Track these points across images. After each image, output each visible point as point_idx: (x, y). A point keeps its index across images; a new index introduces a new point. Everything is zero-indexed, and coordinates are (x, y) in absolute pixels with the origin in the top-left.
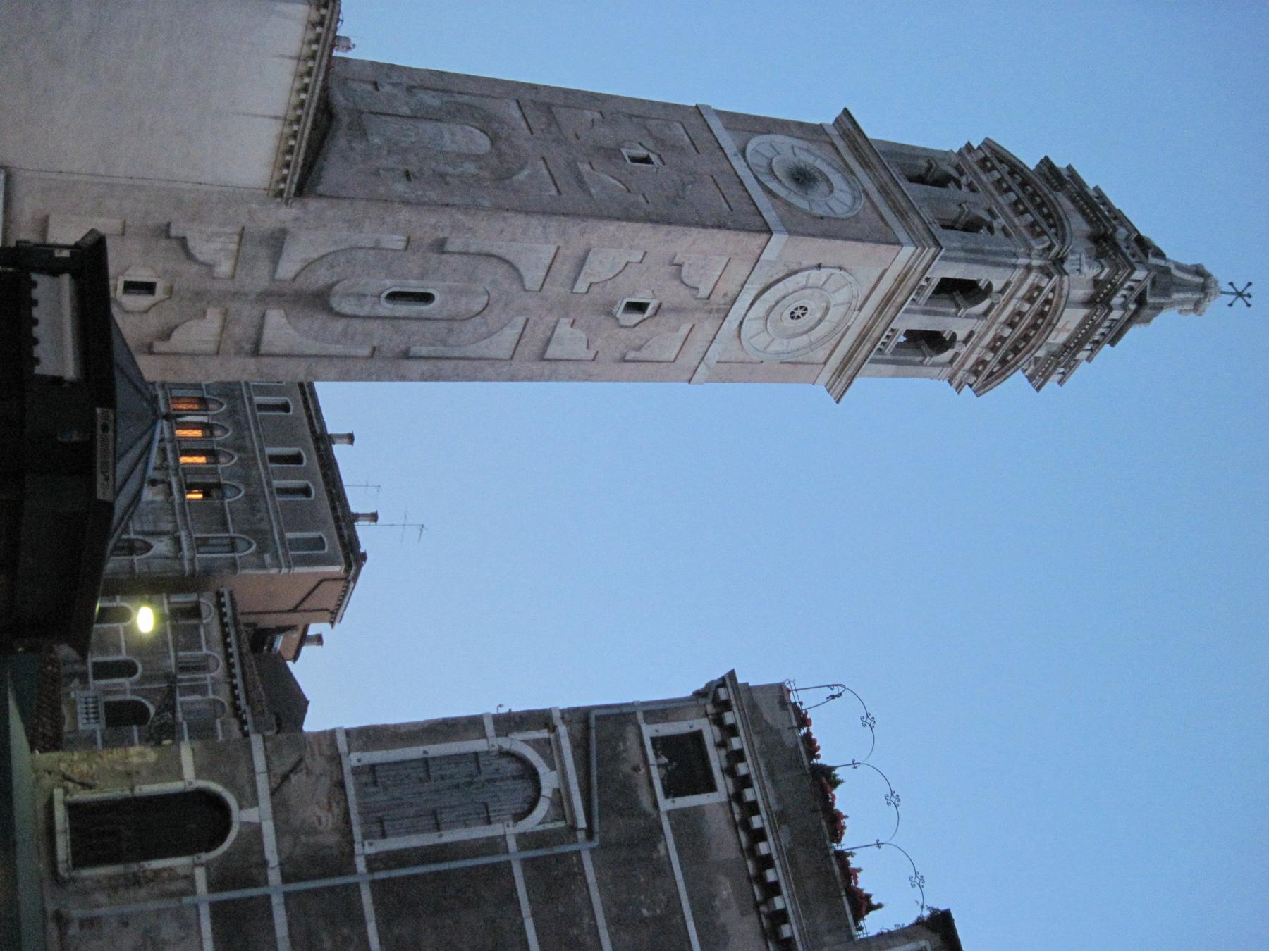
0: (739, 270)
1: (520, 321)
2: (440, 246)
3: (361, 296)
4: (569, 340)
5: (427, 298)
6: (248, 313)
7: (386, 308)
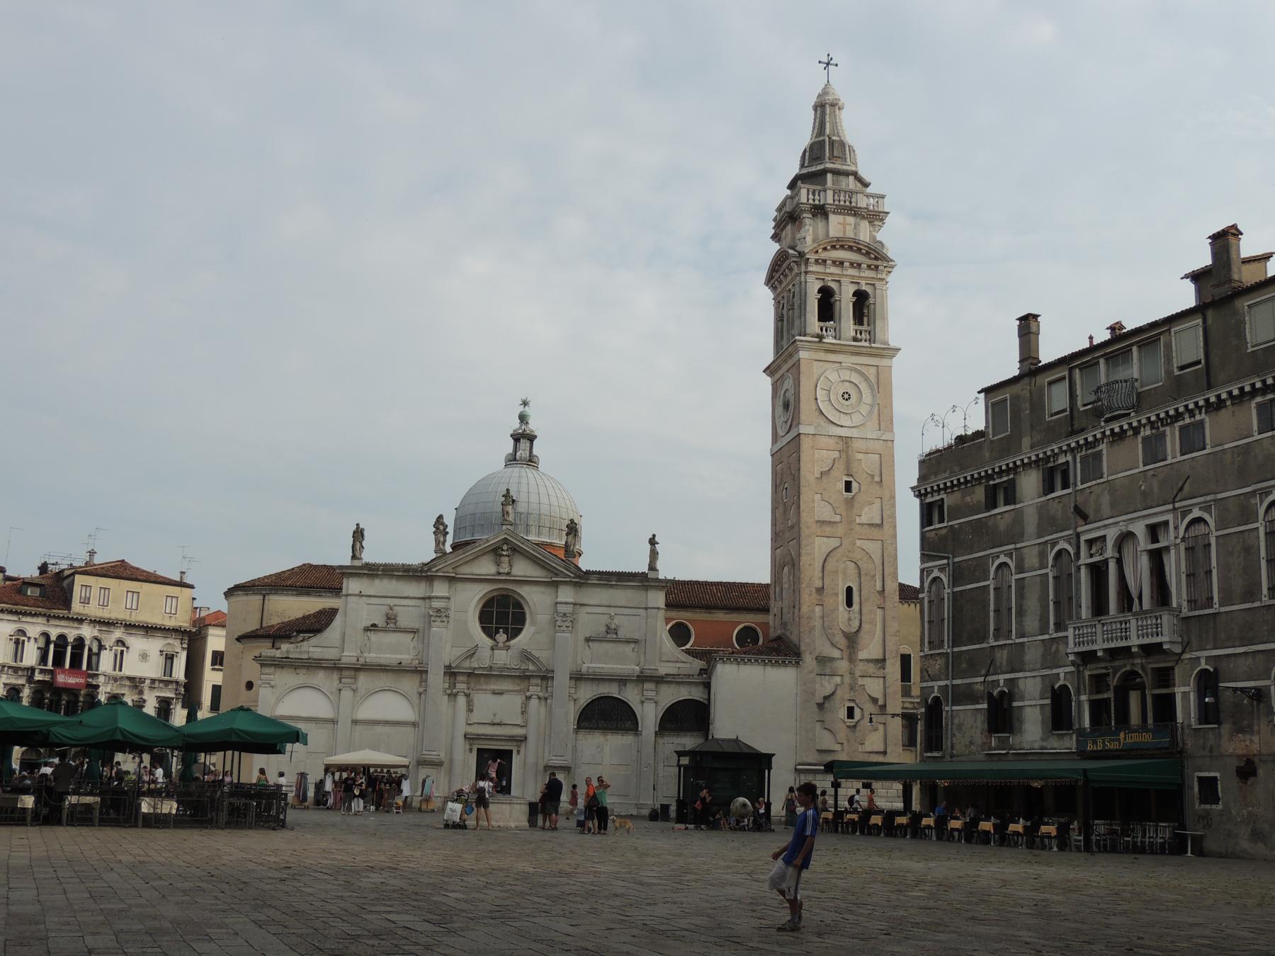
0: (823, 441)
1: (859, 543)
2: (820, 590)
3: (849, 619)
4: (869, 514)
5: (849, 590)
6: (860, 668)
7: (856, 606)
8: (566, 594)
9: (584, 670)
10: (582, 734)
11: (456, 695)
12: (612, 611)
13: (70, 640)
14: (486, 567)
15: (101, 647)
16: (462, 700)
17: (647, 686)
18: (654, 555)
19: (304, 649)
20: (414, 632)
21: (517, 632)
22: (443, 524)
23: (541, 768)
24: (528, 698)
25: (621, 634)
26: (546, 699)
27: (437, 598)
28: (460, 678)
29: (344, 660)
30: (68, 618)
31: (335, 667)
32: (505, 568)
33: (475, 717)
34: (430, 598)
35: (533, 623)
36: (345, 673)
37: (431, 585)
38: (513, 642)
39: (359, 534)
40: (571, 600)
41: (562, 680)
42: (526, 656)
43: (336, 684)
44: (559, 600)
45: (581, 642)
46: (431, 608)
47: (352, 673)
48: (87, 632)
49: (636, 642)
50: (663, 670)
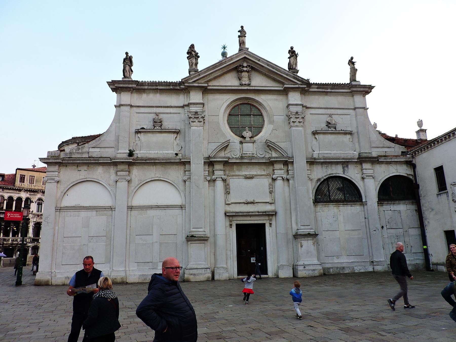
8: (295, 98)
9: (315, 156)
10: (320, 207)
11: (214, 181)
12: (329, 111)
13: (15, 198)
14: (230, 81)
15: (32, 202)
16: (219, 184)
17: (365, 166)
18: (354, 71)
19: (84, 150)
20: (177, 132)
21: (259, 129)
22: (195, 52)
23: (291, 237)
24: (274, 180)
25: (339, 128)
26: (288, 180)
27: (194, 104)
28: (217, 167)
29: (119, 156)
30: (13, 189)
31: (113, 163)
32: (245, 81)
33: (232, 198)
34: (188, 105)
35: (271, 122)
36: (120, 167)
37: (188, 97)
38: (255, 138)
39: (128, 61)
40: (300, 102)
41: (300, 164)
42: (269, 146)
43: (113, 177)
44: (290, 102)
45: (310, 136)
46: (190, 112)
47: (126, 167)
48: (24, 195)
49: (350, 133)
50: (374, 154)
